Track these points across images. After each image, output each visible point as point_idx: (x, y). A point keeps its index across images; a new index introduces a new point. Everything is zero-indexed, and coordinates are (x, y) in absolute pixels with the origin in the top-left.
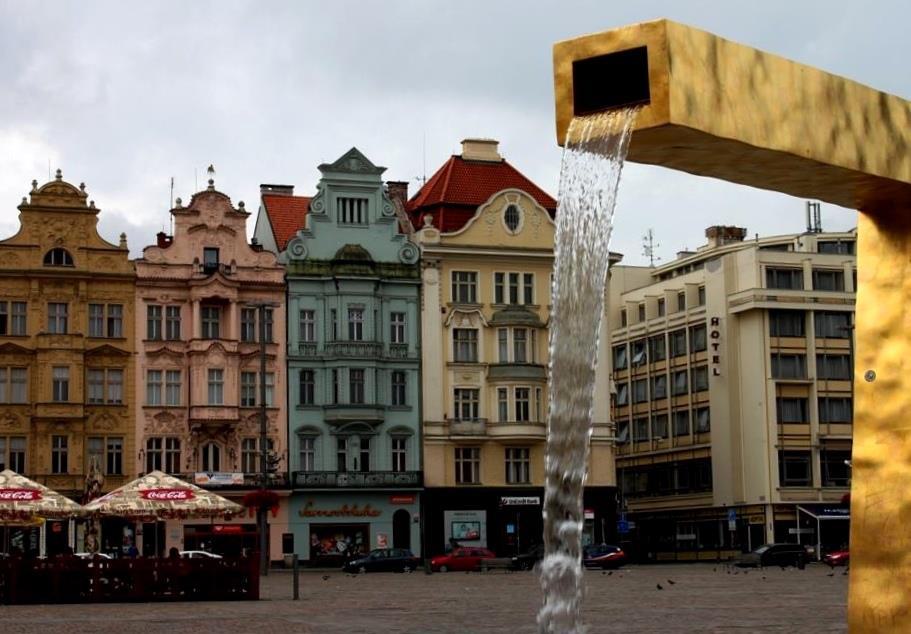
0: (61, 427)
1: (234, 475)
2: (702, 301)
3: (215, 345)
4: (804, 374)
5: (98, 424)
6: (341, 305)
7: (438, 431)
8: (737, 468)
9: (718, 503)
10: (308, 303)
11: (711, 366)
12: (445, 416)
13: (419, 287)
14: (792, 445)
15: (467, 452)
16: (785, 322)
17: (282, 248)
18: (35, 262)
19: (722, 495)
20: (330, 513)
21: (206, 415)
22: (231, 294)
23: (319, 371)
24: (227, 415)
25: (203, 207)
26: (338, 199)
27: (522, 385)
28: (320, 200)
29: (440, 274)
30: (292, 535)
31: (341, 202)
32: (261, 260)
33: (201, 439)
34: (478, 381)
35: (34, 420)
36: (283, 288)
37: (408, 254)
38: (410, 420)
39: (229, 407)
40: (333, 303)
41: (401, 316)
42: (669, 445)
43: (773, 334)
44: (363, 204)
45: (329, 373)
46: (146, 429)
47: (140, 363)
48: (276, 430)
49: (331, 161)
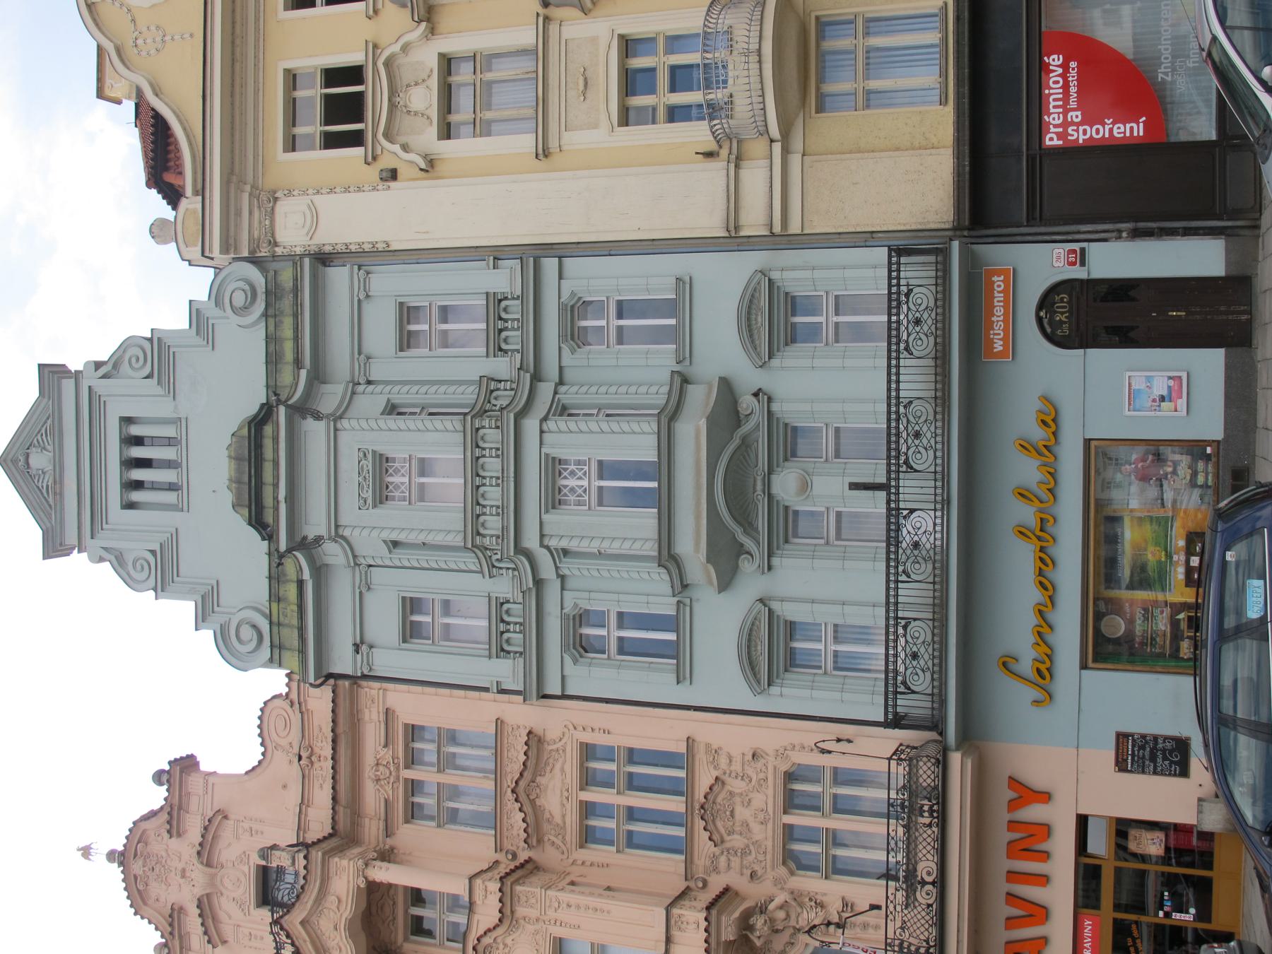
7: (755, 179)
10: (384, 621)
12: (709, 155)
13: (323, 259)
20: (1035, 599)
26: (130, 506)
28: (129, 559)
29: (290, 193)
30: (1121, 737)
31: (136, 496)
32: (284, 742)
34: (594, 40)
36: (346, 687)
37: (239, 299)
38: (722, 283)
41: (407, 313)
44: (135, 430)
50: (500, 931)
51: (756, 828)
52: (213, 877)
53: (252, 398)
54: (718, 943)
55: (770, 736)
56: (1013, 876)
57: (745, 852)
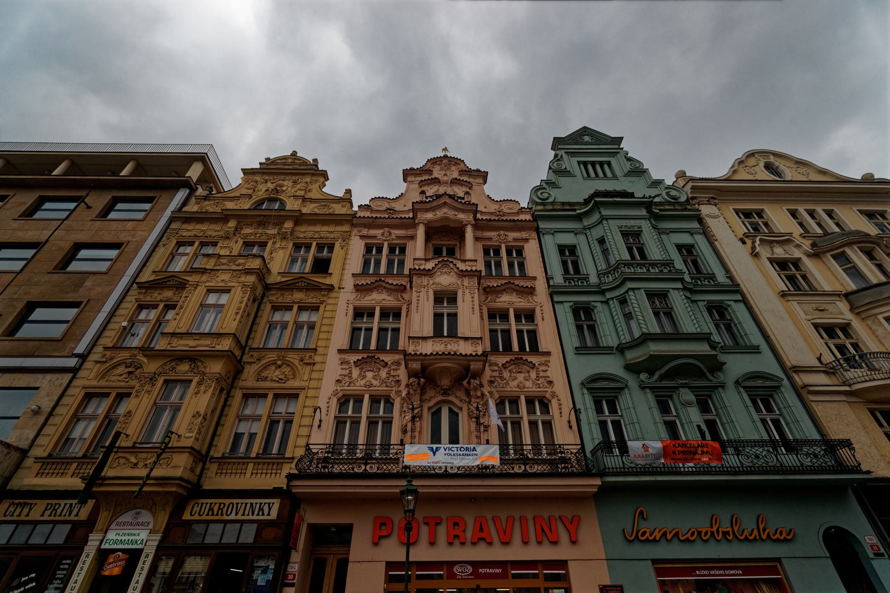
0: (184, 367)
1: (480, 449)
3: (445, 264)
5: (264, 374)
10: (567, 239)
13: (700, 220)
21: (428, 348)
23: (599, 305)
24: (464, 348)
31: (582, 166)
32: (503, 207)
33: (427, 397)
39: (466, 339)
40: (597, 233)
44: (606, 166)
45: (615, 305)
46: (338, 381)
47: (344, 303)
48: (551, 382)
49: (564, 135)
50: (456, 270)
51: (515, 383)
52: (447, 183)
54: (469, 361)
55: (560, 387)
56: (523, 520)
57: (502, 378)
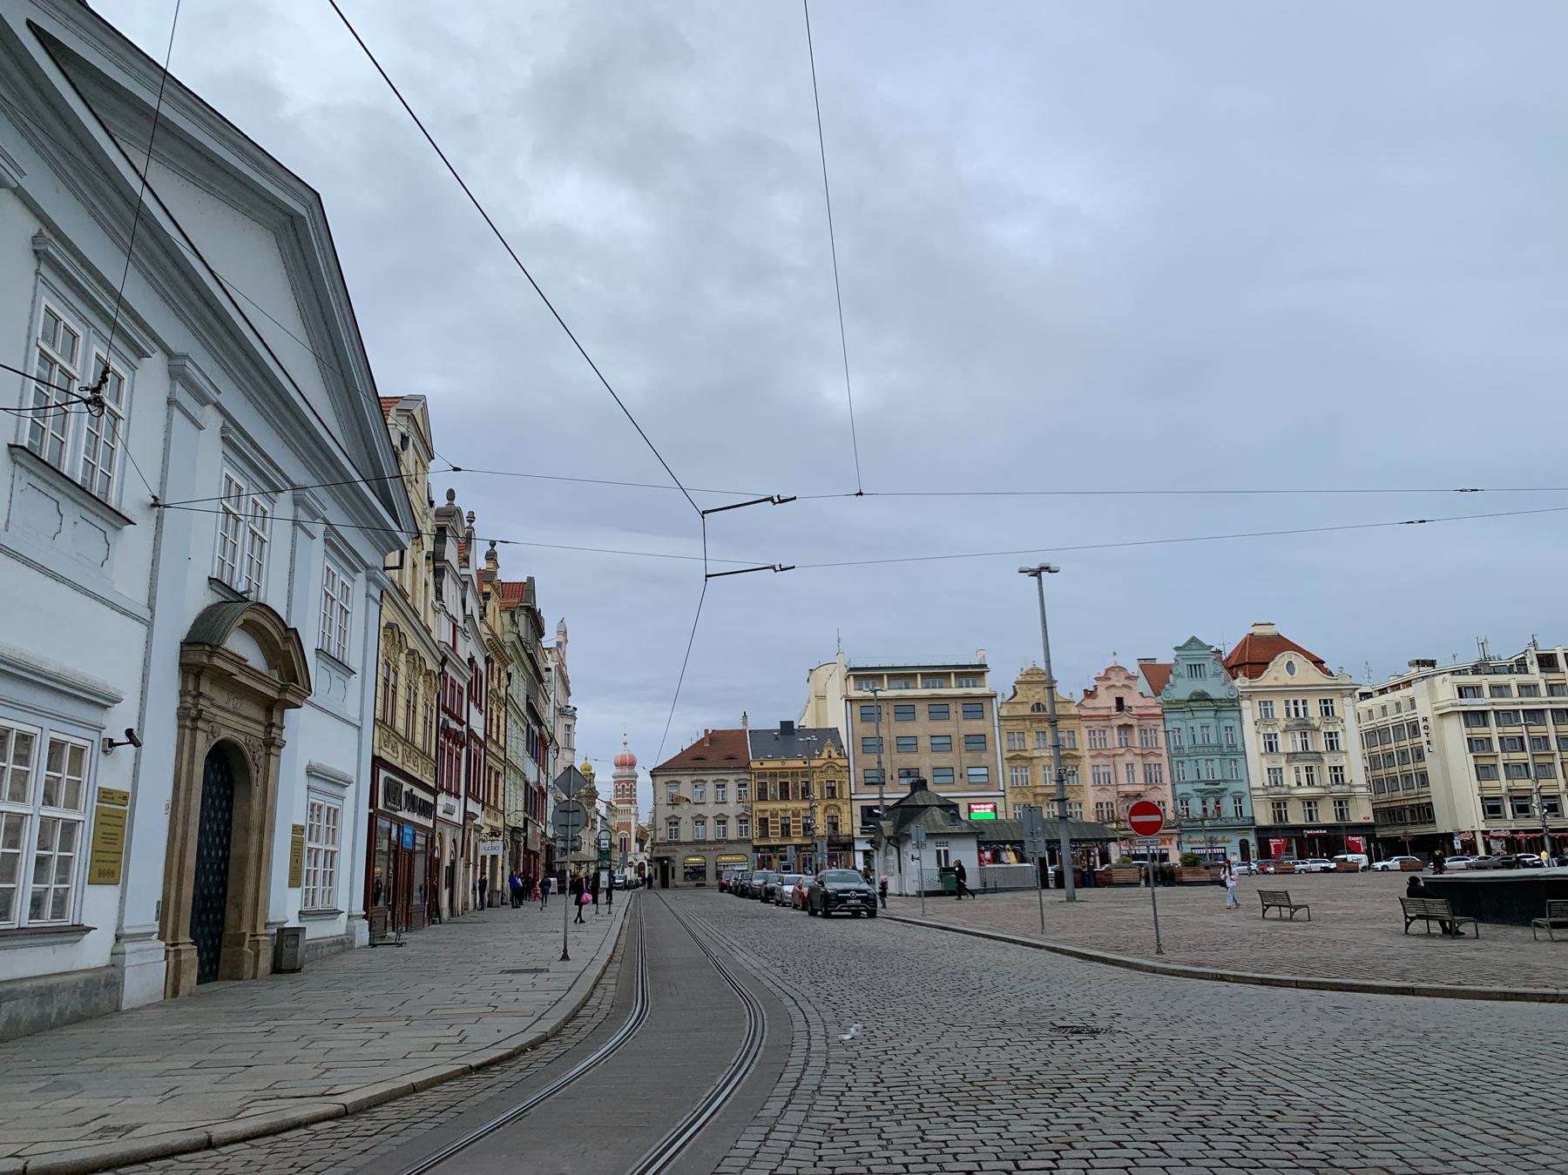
2: (1413, 707)
4: (1491, 750)
6: (1196, 724)
8: (1452, 811)
9: (1441, 831)
11: (1426, 747)
14: (1488, 794)
15: (1279, 805)
16: (1475, 717)
17: (1157, 694)
18: (1026, 711)
19: (1442, 826)
21: (1128, 789)
22: (1133, 722)
25: (1112, 675)
27: (1309, 764)
35: (1035, 795)
36: (1162, 716)
38: (1243, 787)
40: (1191, 723)
42: (1400, 794)
43: (1467, 725)
53: (1214, 694)
55: (1170, 799)
